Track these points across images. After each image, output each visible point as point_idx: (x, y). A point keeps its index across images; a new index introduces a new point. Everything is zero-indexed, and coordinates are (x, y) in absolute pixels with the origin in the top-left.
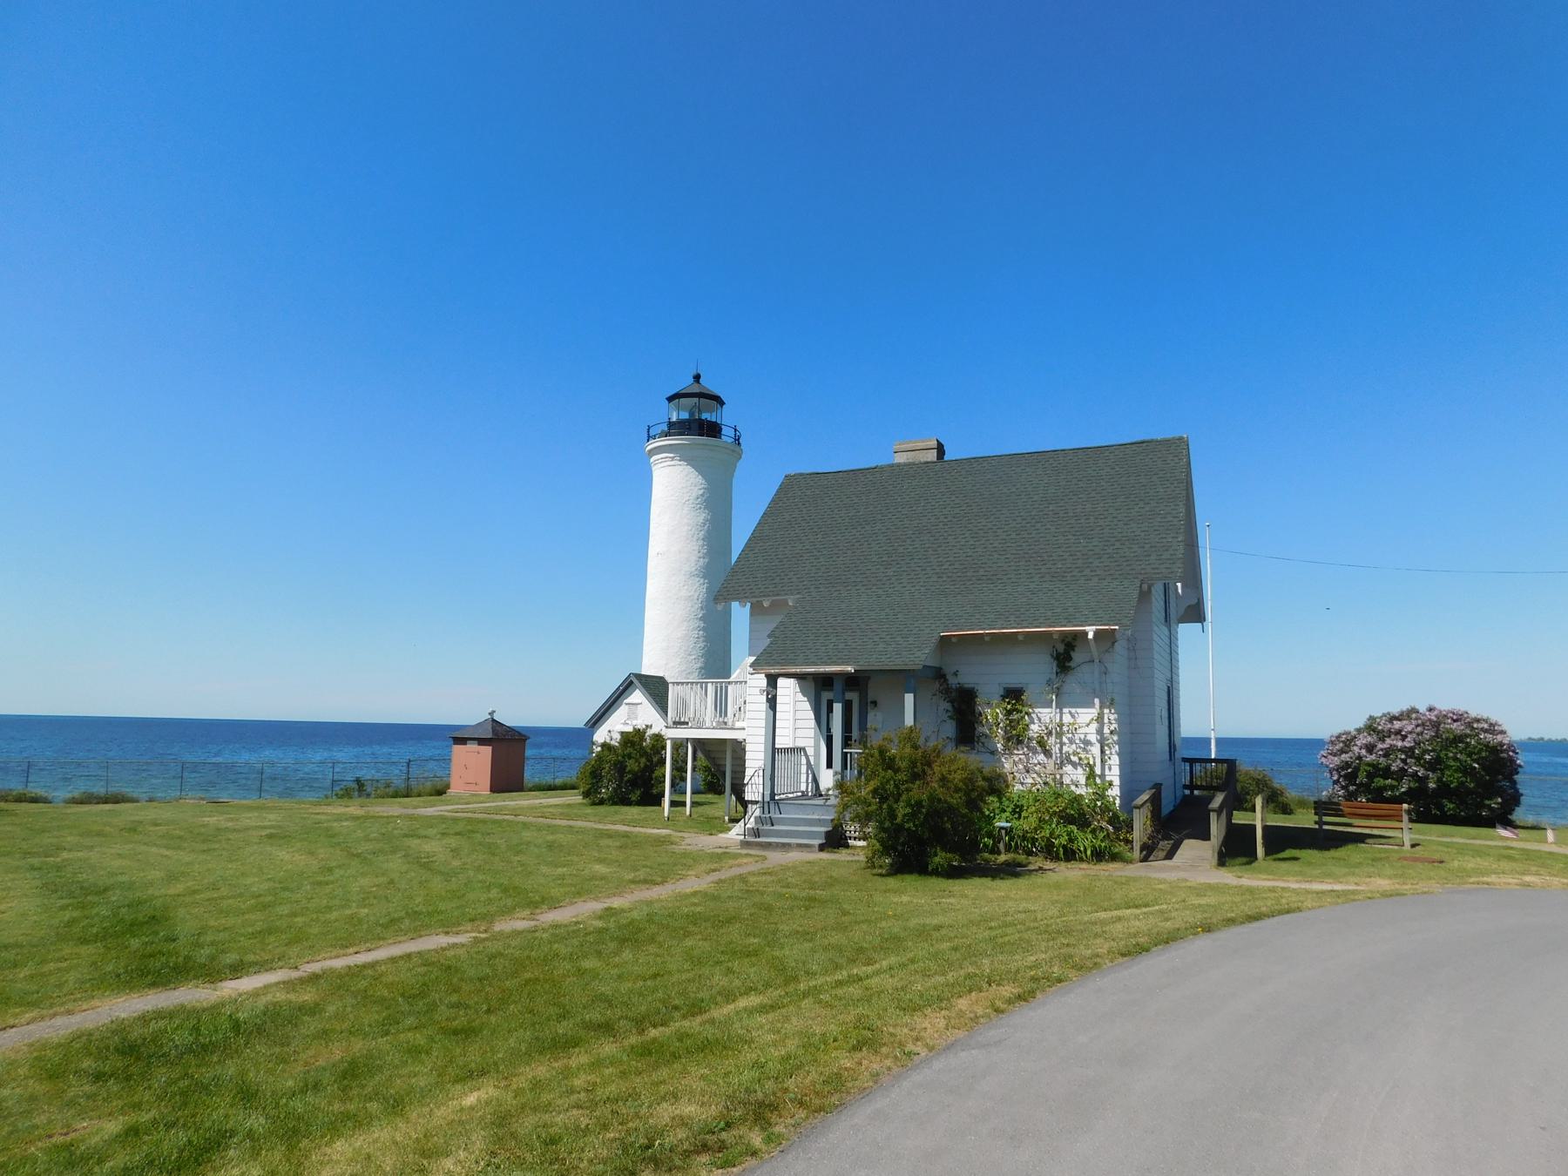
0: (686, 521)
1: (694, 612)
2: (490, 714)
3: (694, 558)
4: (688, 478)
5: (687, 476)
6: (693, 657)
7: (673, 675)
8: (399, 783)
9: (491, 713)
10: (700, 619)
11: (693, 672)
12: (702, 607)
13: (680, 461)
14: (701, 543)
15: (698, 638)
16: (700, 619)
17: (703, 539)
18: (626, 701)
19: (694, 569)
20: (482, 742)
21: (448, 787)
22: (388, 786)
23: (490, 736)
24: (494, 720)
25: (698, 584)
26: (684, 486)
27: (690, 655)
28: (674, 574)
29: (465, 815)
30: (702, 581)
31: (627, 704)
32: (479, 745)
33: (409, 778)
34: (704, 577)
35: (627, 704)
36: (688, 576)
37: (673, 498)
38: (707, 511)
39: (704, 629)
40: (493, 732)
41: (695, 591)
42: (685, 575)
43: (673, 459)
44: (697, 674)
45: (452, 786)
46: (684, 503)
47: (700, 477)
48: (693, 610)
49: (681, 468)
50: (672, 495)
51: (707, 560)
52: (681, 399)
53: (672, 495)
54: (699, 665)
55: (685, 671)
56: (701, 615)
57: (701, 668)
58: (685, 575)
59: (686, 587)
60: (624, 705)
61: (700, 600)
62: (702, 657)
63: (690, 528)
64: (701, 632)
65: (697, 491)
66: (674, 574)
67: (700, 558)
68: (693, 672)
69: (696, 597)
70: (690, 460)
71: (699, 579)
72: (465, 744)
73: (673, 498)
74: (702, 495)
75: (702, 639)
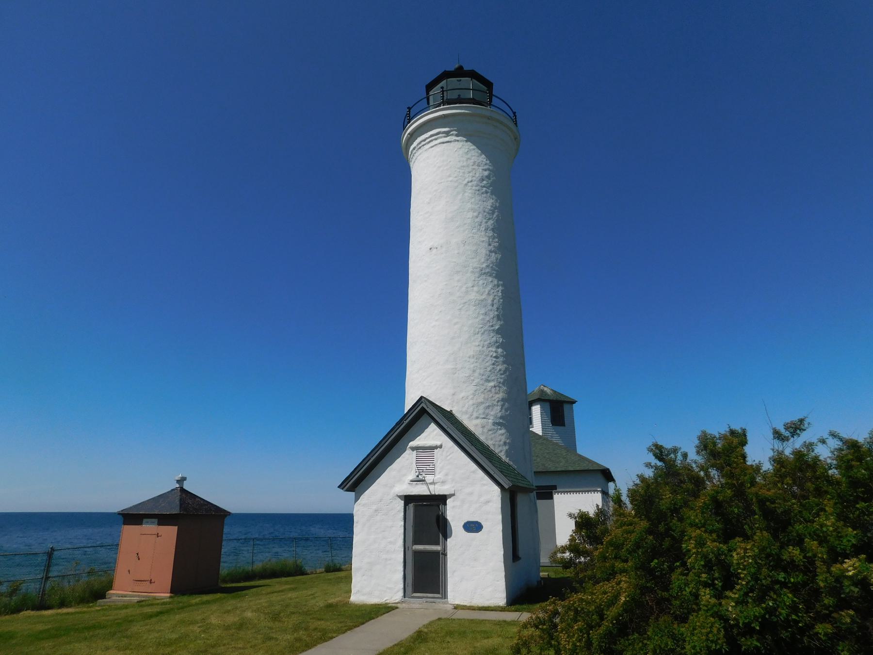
0: (469, 206)
1: (489, 321)
2: (178, 481)
3: (483, 251)
4: (469, 156)
5: (467, 153)
6: (492, 384)
7: (464, 409)
8: (32, 588)
9: (181, 481)
10: (498, 332)
11: (493, 405)
12: (498, 316)
13: (457, 135)
14: (490, 233)
15: (496, 357)
16: (498, 332)
17: (493, 230)
18: (413, 444)
19: (484, 265)
20: (163, 520)
21: (110, 585)
22: (14, 591)
23: (176, 511)
24: (183, 490)
25: (490, 286)
26: (465, 164)
27: (488, 381)
28: (458, 272)
29: (146, 594)
30: (496, 282)
31: (413, 449)
32: (159, 524)
33: (47, 578)
34: (498, 277)
35: (413, 449)
36: (477, 275)
37: (451, 179)
38: (494, 197)
39: (501, 346)
40: (181, 505)
41: (489, 294)
42: (472, 272)
43: (447, 134)
44: (499, 408)
45: (117, 583)
46: (466, 185)
47: (483, 156)
48: (488, 318)
49: (460, 144)
50: (449, 176)
51: (499, 256)
52: (448, 80)
53: (449, 176)
54: (501, 395)
55: (482, 403)
56: (497, 327)
57: (503, 400)
58: (472, 272)
59: (475, 289)
60: (408, 451)
61: (495, 306)
62: (503, 384)
63: (475, 214)
64: (500, 350)
65: (480, 172)
66: (458, 272)
67: (491, 251)
68: (493, 405)
69: (490, 301)
70: (470, 136)
71: (490, 279)
72: (141, 524)
73: (451, 179)
74: (488, 177)
75: (501, 359)
